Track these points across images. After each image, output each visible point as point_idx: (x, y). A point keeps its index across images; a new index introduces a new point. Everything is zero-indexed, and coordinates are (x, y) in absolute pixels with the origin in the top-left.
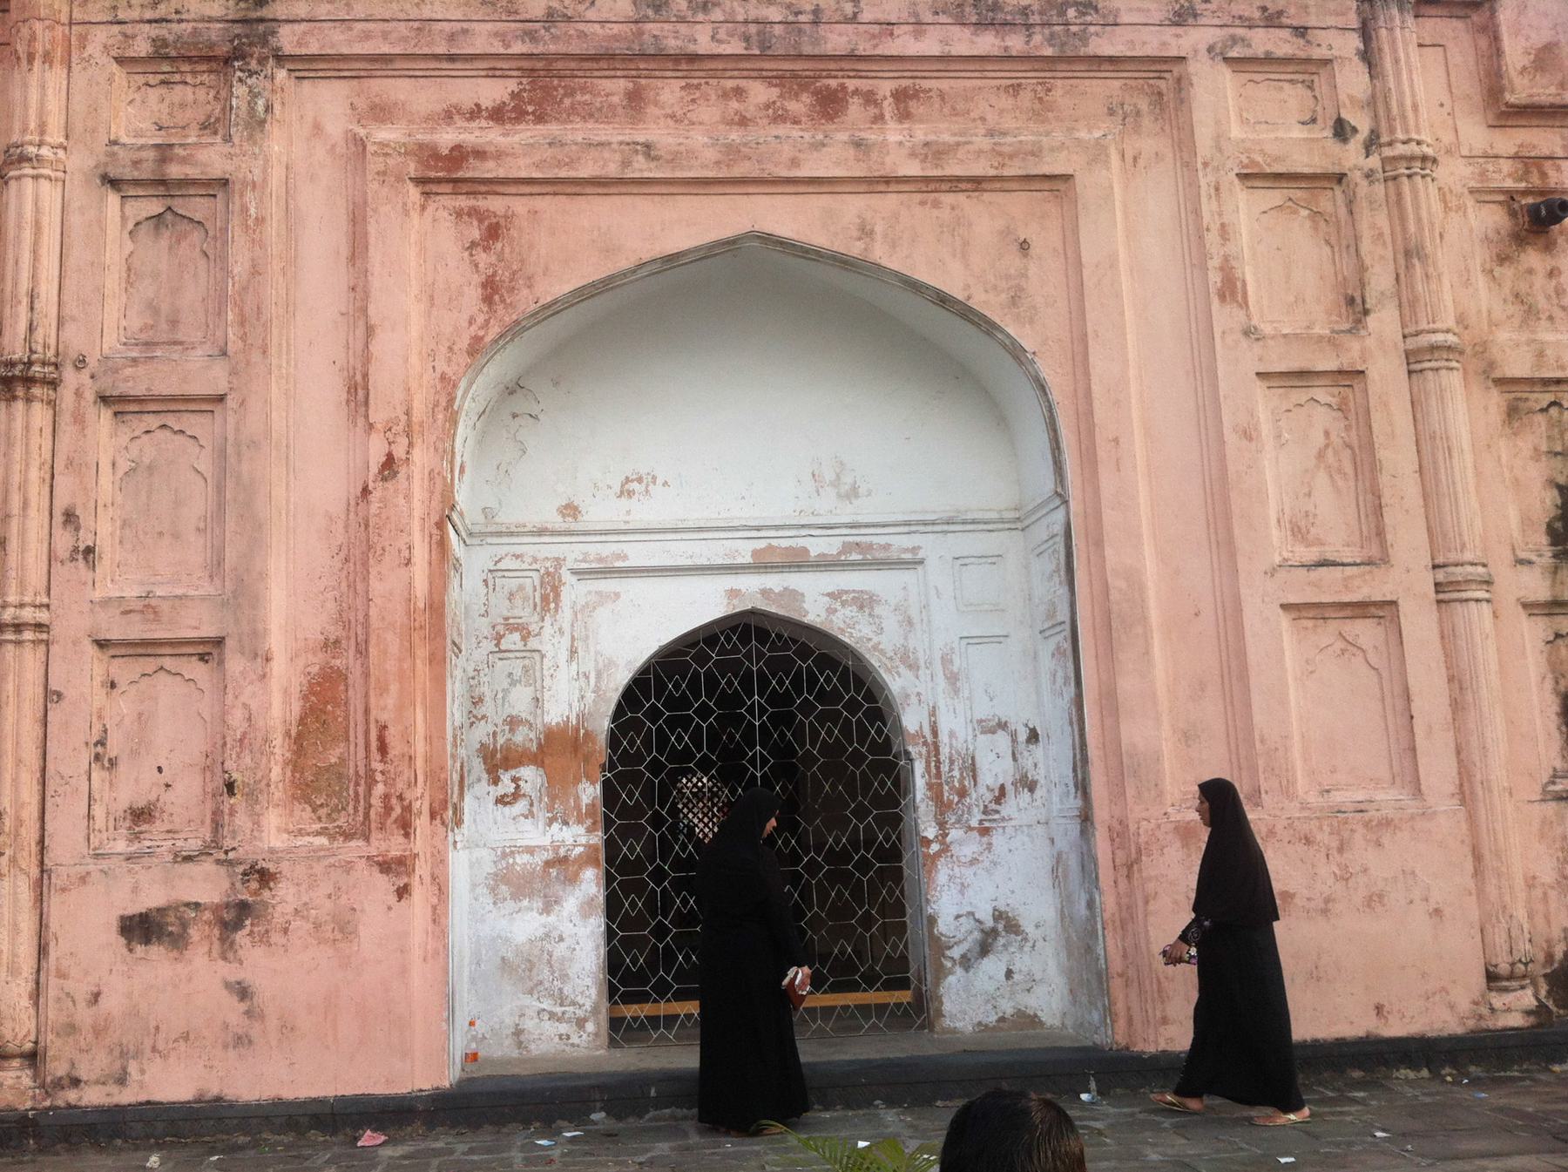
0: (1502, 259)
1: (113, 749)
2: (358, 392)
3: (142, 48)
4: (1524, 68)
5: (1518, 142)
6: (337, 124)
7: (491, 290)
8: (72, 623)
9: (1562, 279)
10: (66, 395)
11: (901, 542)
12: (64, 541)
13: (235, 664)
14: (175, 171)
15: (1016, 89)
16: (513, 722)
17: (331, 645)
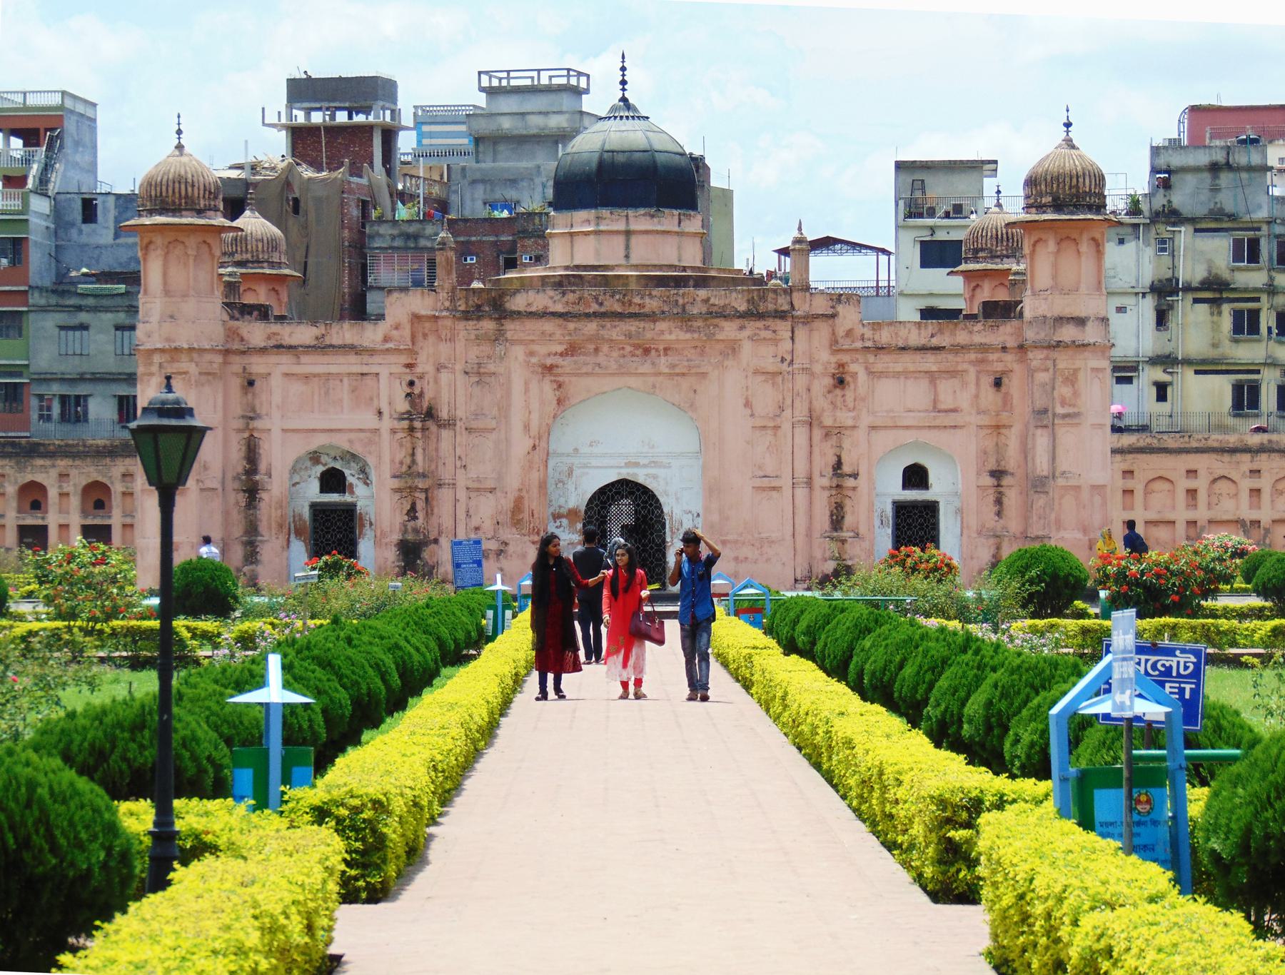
0: (829, 392)
1: (471, 512)
2: (527, 427)
3: (473, 337)
6: (521, 357)
7: (559, 402)
8: (462, 481)
10: (458, 428)
11: (665, 461)
12: (458, 464)
13: (499, 494)
14: (482, 370)
15: (696, 347)
16: (560, 507)
17: (520, 490)
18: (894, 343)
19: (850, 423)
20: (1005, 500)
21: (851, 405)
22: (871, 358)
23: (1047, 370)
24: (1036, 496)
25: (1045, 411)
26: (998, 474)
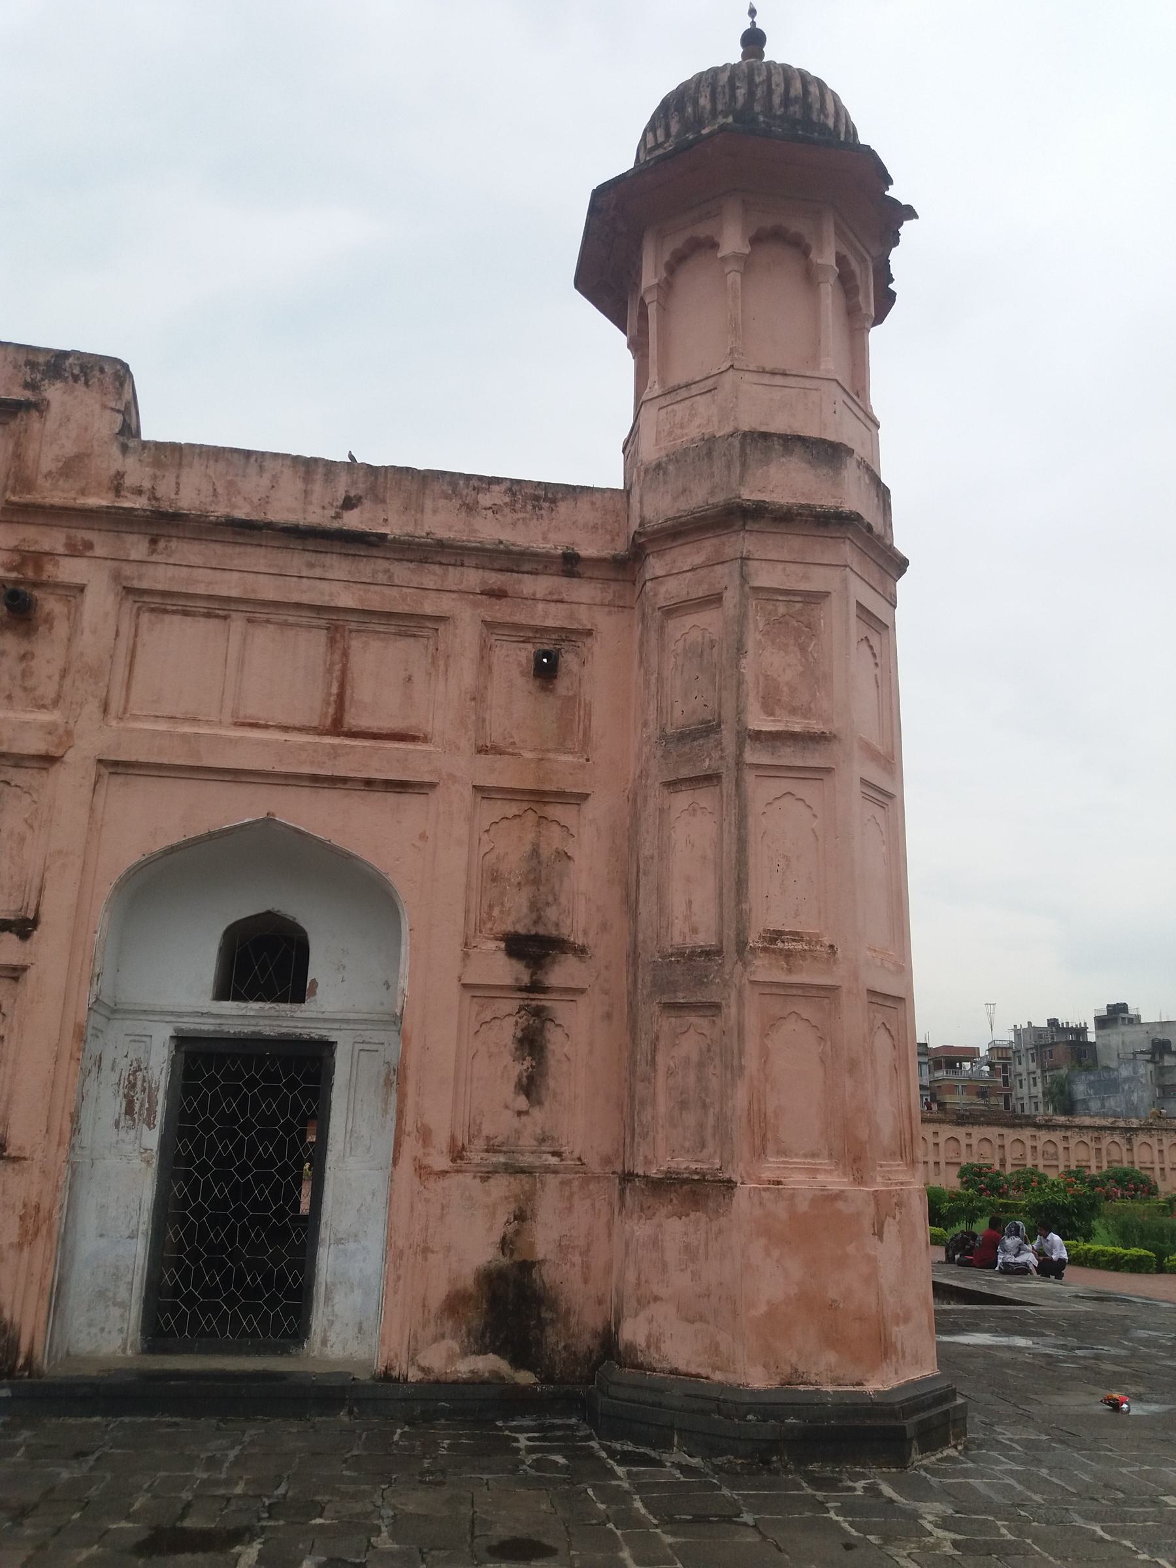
4: (50, 473)
5: (21, 537)
9: (33, 663)
18: (220, 510)
19: (34, 744)
20: (555, 1039)
21: (48, 690)
22: (137, 547)
23: (714, 600)
24: (668, 1024)
25: (709, 729)
26: (533, 948)
